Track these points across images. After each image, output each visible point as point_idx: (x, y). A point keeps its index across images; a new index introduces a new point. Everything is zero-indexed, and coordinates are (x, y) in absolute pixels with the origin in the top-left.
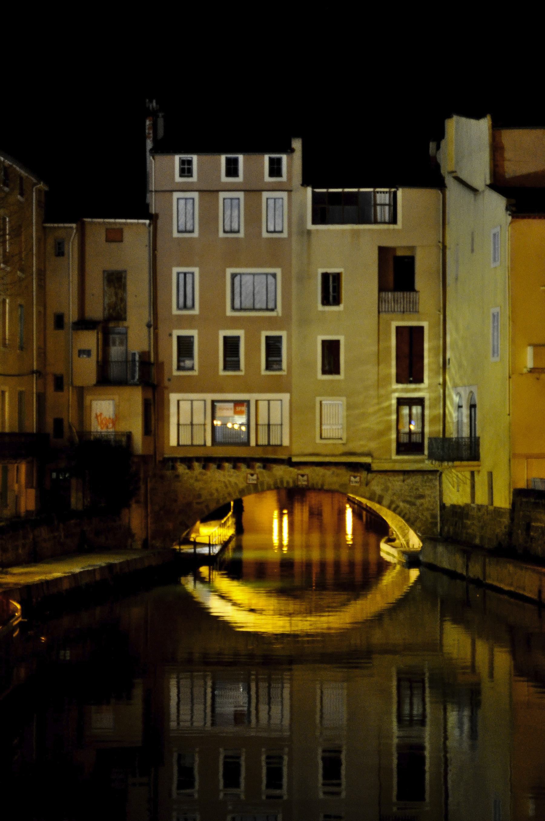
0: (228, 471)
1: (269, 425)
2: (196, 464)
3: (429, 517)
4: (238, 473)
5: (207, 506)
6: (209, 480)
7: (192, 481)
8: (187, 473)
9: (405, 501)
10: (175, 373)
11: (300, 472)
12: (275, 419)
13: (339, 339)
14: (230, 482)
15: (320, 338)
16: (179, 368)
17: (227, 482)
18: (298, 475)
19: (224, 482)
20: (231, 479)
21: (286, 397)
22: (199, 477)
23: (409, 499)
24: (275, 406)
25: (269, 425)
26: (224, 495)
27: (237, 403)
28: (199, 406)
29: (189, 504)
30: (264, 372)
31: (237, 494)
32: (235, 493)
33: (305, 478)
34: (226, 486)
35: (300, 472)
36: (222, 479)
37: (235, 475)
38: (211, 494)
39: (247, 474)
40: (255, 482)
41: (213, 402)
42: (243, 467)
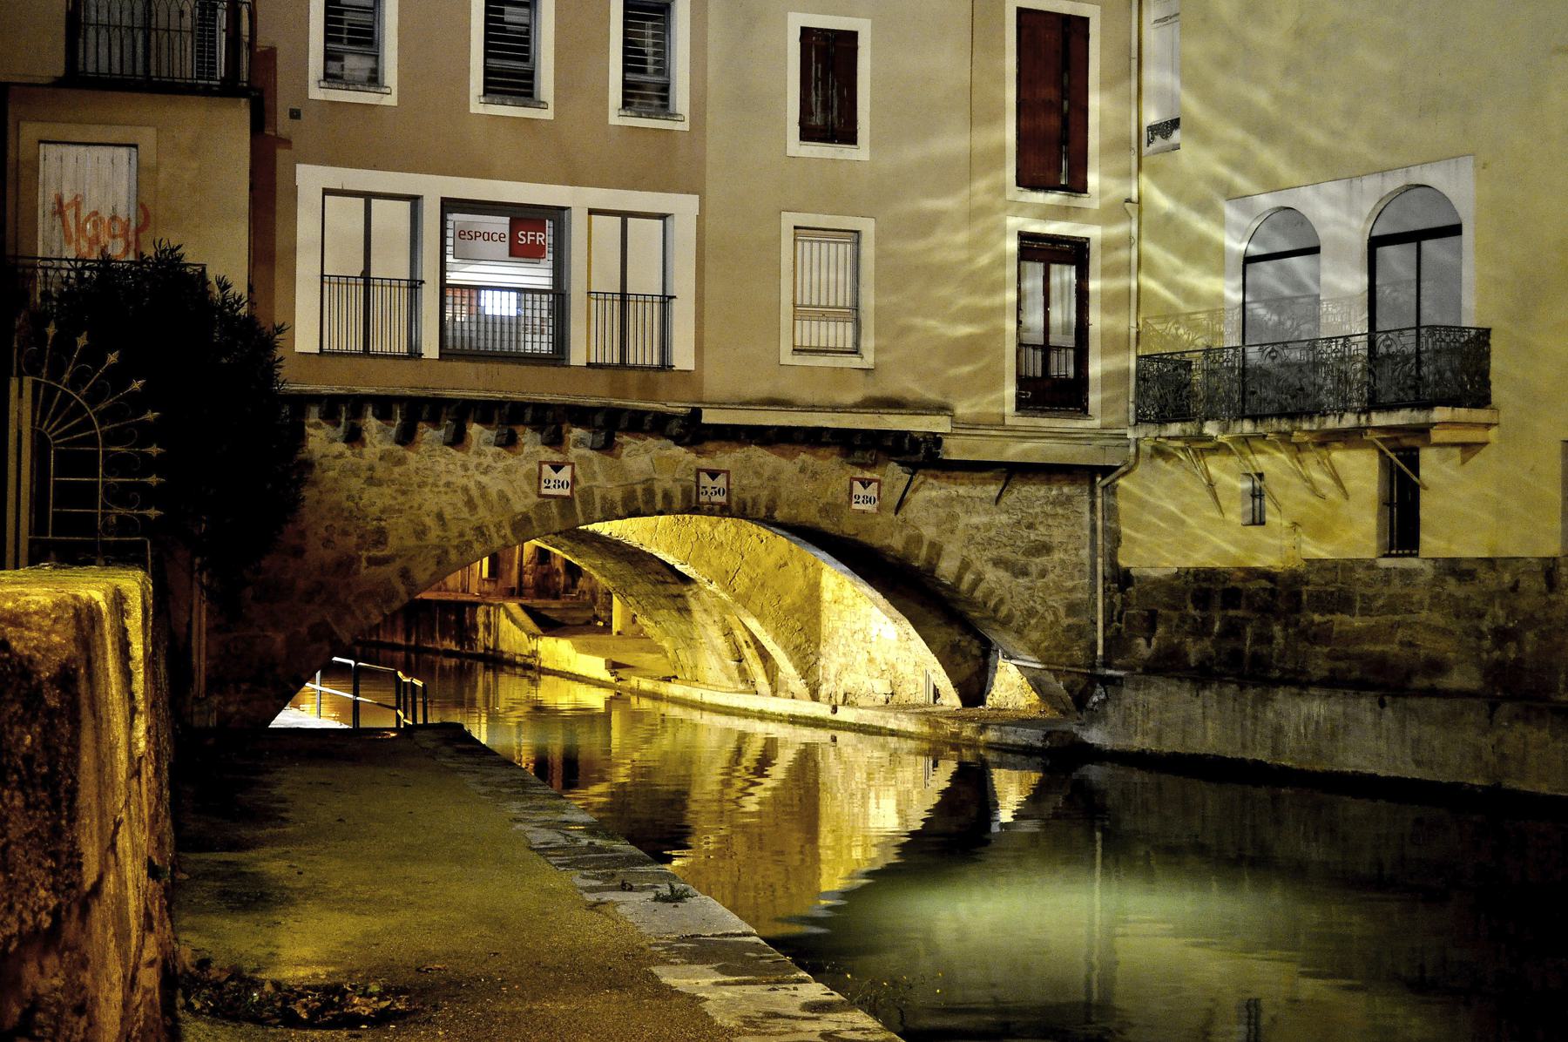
0: (479, 454)
1: (624, 296)
2: (371, 423)
3: (1062, 612)
4: (511, 460)
5: (405, 574)
6: (416, 479)
7: (355, 484)
8: (341, 455)
9: (998, 563)
10: (316, 93)
11: (704, 462)
12: (644, 280)
13: (854, 29)
14: (482, 487)
15: (796, 22)
16: (330, 78)
17: (475, 493)
18: (699, 471)
19: (466, 490)
20: (484, 479)
21: (684, 207)
22: (380, 472)
23: (1006, 553)
24: (644, 234)
25: (624, 296)
26: (461, 535)
27: (524, 217)
28: (391, 218)
29: (346, 565)
30: (616, 117)
31: (507, 531)
32: (499, 526)
33: (721, 482)
34: (471, 504)
35: (704, 462)
36: (459, 480)
37: (500, 465)
38: (421, 533)
39: (541, 463)
40: (566, 492)
41: (450, 205)
42: (529, 440)
